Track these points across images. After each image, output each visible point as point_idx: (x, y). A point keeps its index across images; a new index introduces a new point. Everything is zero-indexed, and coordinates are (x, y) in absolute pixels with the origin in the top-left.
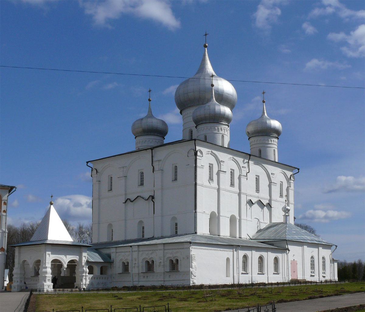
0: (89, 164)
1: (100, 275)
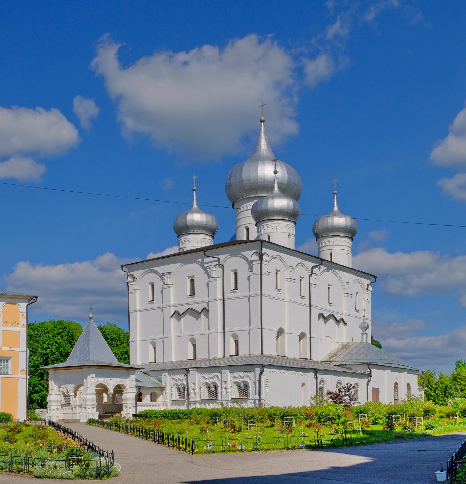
0: (124, 268)
1: (150, 402)
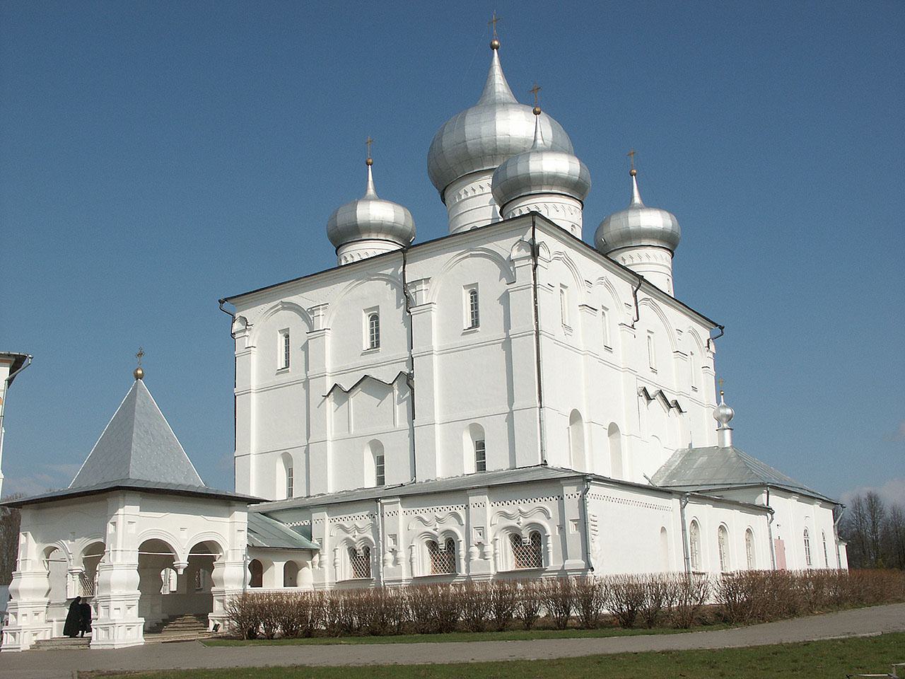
0: (226, 305)
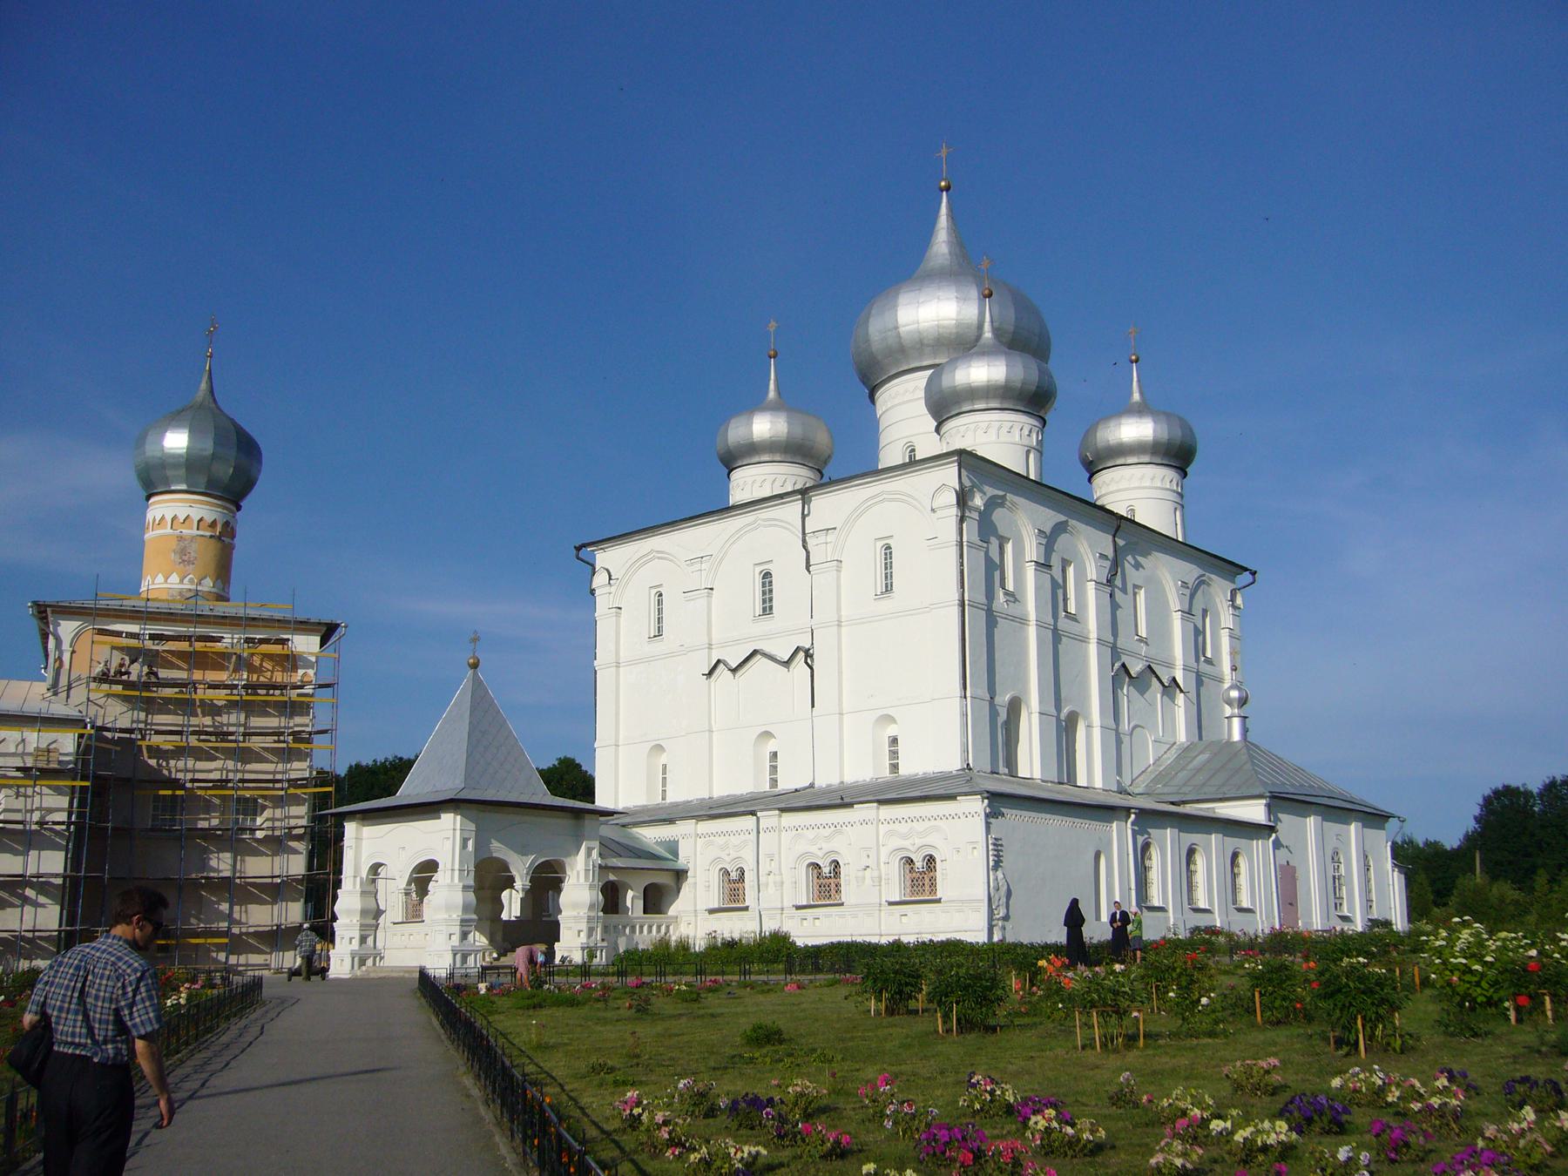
0: (582, 554)
